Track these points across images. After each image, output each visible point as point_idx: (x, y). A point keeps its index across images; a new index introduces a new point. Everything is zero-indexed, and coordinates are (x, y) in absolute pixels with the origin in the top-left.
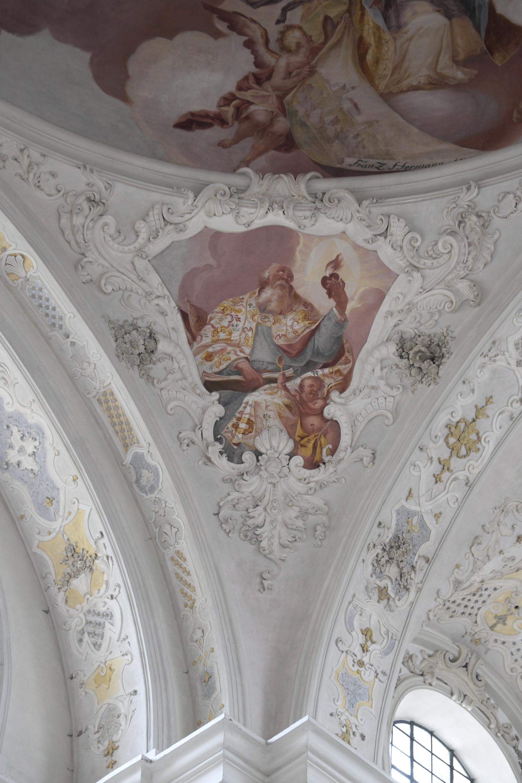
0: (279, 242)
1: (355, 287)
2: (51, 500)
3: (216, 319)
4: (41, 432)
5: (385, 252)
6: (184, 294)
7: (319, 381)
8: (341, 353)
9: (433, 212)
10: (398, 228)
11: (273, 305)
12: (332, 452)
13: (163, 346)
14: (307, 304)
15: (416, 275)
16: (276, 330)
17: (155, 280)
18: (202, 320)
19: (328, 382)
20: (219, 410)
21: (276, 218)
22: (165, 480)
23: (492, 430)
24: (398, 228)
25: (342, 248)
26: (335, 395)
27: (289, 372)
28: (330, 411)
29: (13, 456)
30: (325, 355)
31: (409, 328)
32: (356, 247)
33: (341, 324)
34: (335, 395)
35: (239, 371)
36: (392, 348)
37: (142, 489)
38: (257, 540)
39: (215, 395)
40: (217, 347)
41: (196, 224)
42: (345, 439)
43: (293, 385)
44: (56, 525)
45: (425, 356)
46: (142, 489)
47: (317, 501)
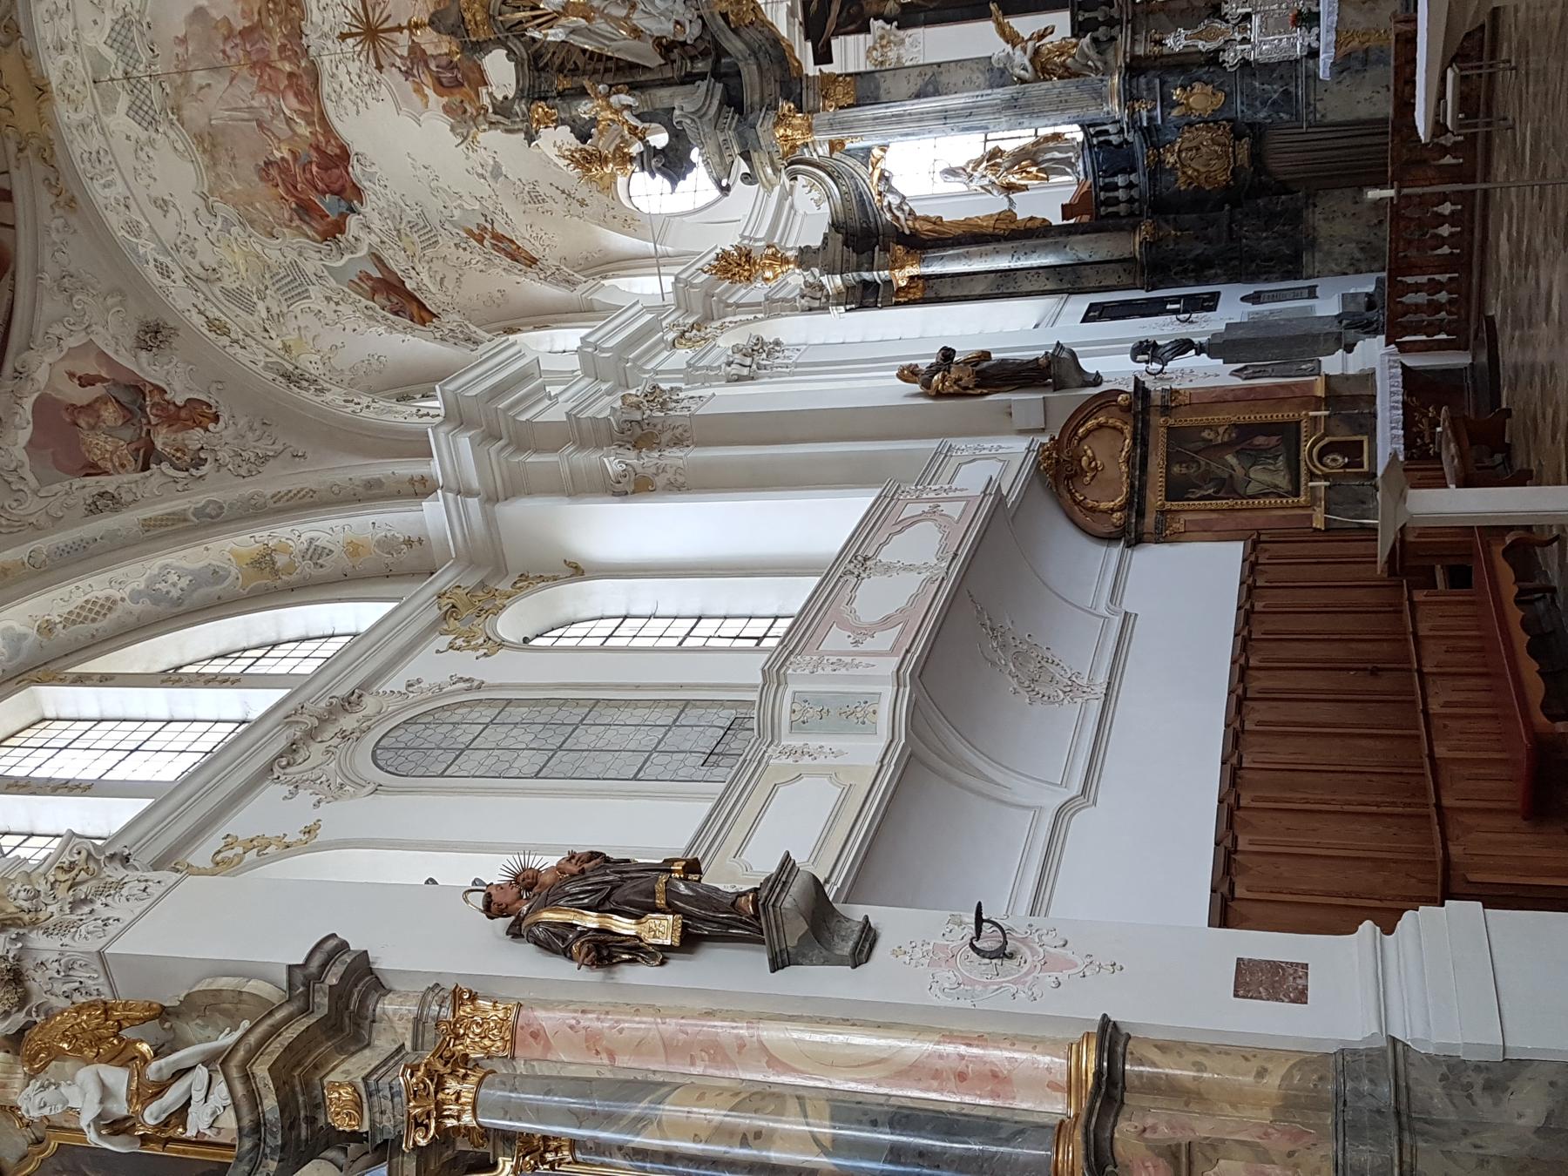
0: (45, 407)
1: (91, 368)
2: (215, 572)
3: (95, 456)
4: (166, 566)
5: (72, 342)
6: (74, 473)
7: (153, 405)
8: (138, 389)
9: (50, 306)
10: (58, 330)
11: (92, 421)
12: (210, 406)
13: (111, 489)
14: (96, 400)
15: (94, 327)
16: (111, 423)
17: (57, 487)
18: (94, 465)
19: (157, 398)
20: (164, 466)
21: (28, 404)
22: (214, 496)
23: (214, 313)
24: (58, 330)
25: (62, 368)
26: (167, 397)
27: (144, 421)
28: (179, 402)
29: (175, 593)
30: (135, 397)
31: (130, 342)
32: (62, 359)
33: (116, 383)
34: (167, 397)
35: (138, 450)
36: (144, 353)
37: (218, 515)
38: (266, 458)
39: (153, 466)
40: (115, 459)
41: (20, 454)
42: (203, 398)
43: (154, 420)
44: (234, 571)
45: (154, 336)
46: (218, 515)
47: (242, 422)
